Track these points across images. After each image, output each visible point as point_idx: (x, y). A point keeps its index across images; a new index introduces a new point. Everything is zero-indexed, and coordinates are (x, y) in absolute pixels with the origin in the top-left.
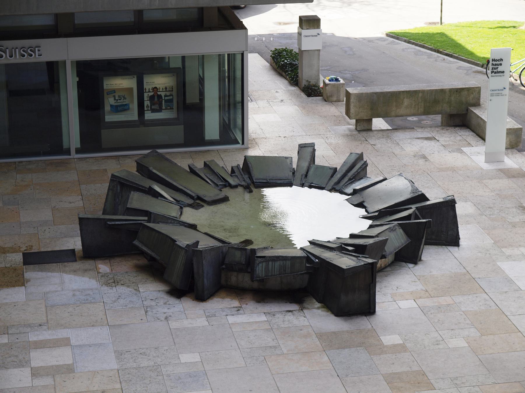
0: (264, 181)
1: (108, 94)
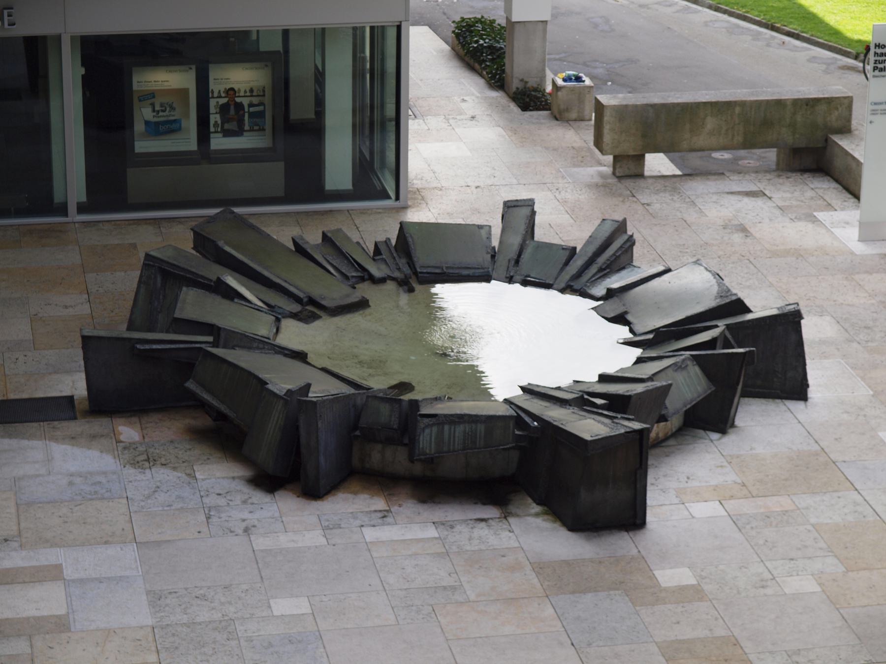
1: (140, 101)
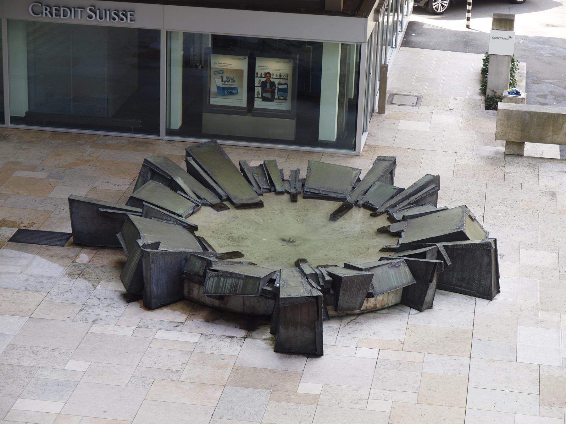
0: (316, 192)
1: (215, 74)
